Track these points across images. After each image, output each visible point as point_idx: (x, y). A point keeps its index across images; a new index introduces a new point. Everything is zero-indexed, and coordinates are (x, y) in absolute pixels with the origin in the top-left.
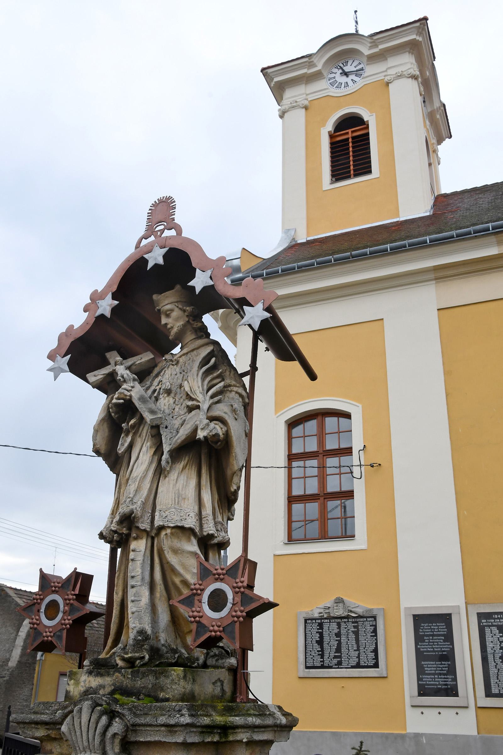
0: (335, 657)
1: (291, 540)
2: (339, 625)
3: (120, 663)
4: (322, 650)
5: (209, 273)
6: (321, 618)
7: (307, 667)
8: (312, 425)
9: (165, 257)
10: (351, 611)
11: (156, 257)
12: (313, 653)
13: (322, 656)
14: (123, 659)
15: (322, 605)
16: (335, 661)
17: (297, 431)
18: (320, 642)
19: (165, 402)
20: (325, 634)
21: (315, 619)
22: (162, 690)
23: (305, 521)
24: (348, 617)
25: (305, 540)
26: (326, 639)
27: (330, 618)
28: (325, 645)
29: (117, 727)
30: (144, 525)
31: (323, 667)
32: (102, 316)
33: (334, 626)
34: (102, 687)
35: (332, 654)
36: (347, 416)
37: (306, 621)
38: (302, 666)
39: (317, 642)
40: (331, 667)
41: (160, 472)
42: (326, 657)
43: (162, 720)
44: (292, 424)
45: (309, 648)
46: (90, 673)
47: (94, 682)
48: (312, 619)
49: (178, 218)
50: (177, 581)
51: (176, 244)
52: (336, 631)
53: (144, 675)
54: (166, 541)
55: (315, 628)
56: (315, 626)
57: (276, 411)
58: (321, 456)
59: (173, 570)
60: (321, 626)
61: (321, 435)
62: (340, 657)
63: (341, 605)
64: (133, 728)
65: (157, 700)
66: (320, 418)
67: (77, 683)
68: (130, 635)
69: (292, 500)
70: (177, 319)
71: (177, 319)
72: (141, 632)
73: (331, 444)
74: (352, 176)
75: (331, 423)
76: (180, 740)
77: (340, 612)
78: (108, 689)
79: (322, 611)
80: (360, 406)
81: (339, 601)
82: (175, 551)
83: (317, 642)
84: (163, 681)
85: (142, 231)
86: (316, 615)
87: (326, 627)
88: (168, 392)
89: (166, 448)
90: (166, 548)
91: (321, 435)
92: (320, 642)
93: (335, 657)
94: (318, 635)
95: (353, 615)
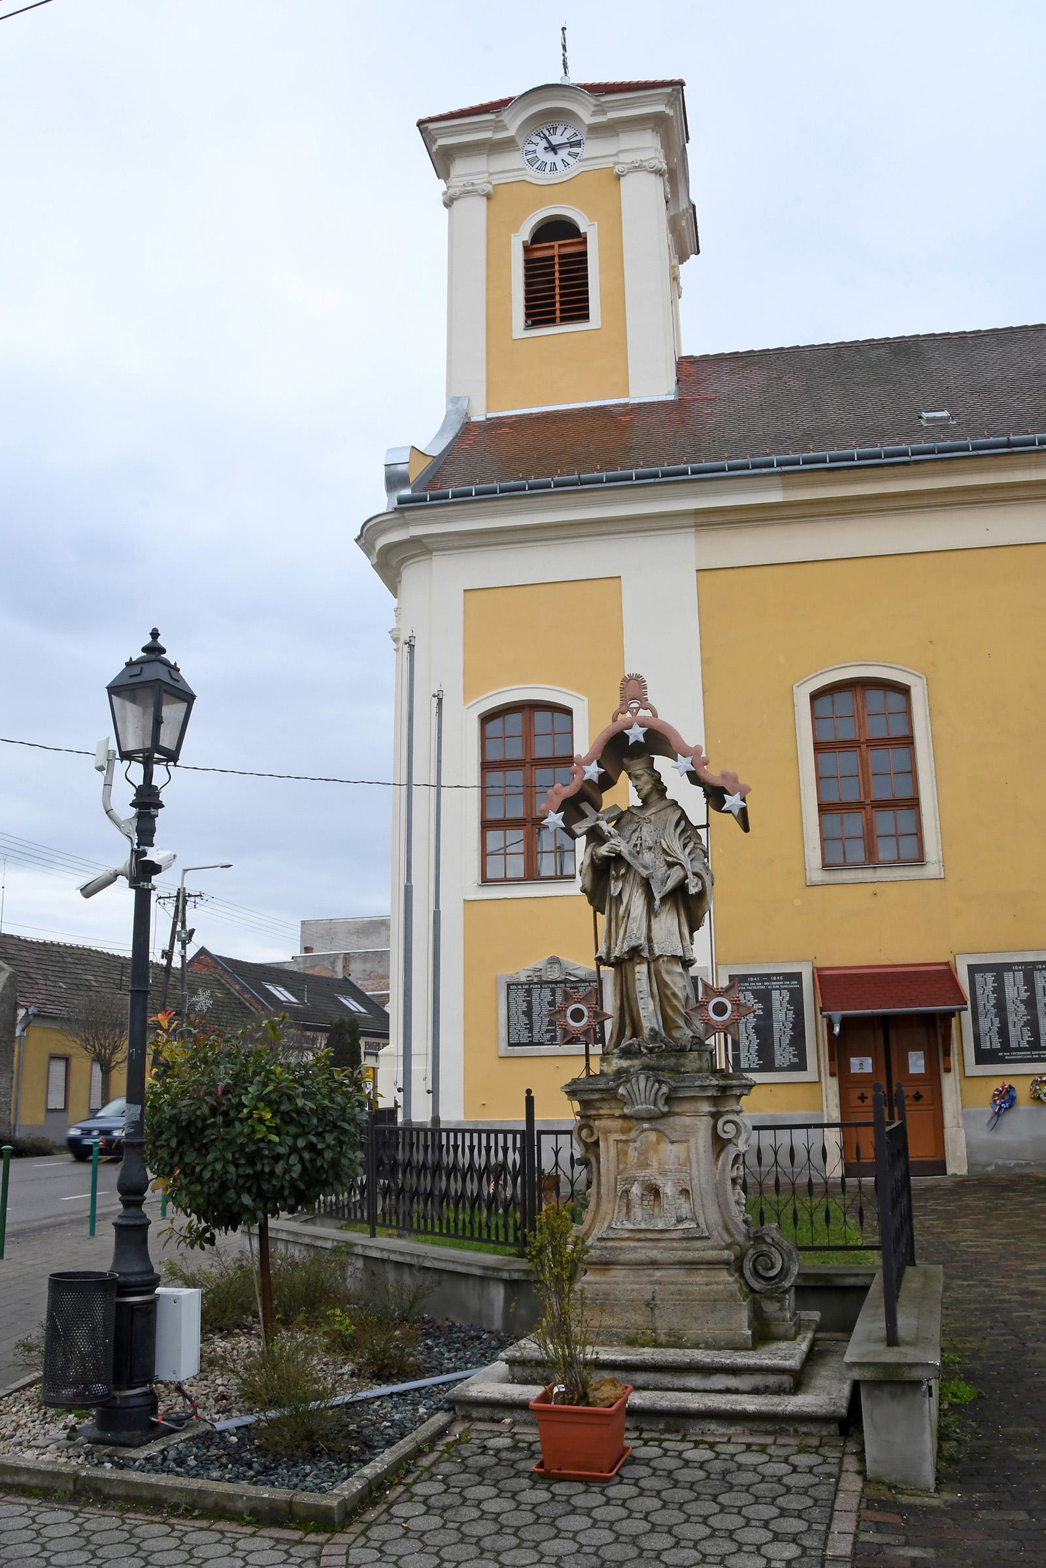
0: (548, 1031)
1: (485, 881)
2: (553, 992)
3: (645, 1051)
4: (531, 1023)
5: (690, 759)
6: (530, 983)
7: (510, 1045)
8: (515, 720)
9: (645, 735)
10: (570, 974)
11: (636, 734)
12: (518, 1027)
13: (531, 1030)
14: (646, 1048)
15: (531, 966)
16: (548, 1036)
17: (494, 726)
18: (528, 1013)
19: (648, 857)
20: (535, 1003)
21: (522, 984)
22: (683, 1066)
23: (505, 854)
24: (565, 981)
25: (506, 881)
26: (536, 1009)
27: (542, 983)
28: (535, 1017)
29: (665, 1089)
30: (645, 954)
31: (531, 1043)
32: (589, 781)
33: (547, 993)
34: (631, 1066)
35: (544, 1028)
36: (568, 712)
37: (509, 986)
38: (504, 1044)
39: (524, 1012)
40: (542, 1044)
41: (651, 912)
42: (535, 1032)
43: (698, 1083)
44: (487, 718)
45: (514, 1020)
46: (621, 1058)
47: (625, 1063)
48: (517, 985)
49: (652, 698)
50: (669, 993)
51: (653, 723)
52: (550, 998)
53: (666, 1058)
54: (663, 966)
55: (521, 994)
56: (522, 993)
57: (466, 699)
58: (528, 765)
59: (666, 985)
60: (529, 992)
61: (528, 736)
62: (554, 1031)
63: (556, 966)
64: (674, 1089)
65: (680, 1072)
66: (527, 711)
67: (610, 1064)
68: (646, 1032)
69: (487, 825)
70: (646, 783)
71: (646, 783)
72: (652, 1030)
73: (542, 749)
74: (558, 320)
75: (541, 719)
76: (710, 1094)
77: (555, 975)
78: (637, 1068)
79: (530, 973)
80: (586, 699)
81: (554, 961)
82: (669, 972)
83: (524, 1012)
84: (682, 1061)
85: (616, 704)
86: (523, 979)
87: (535, 994)
88: (650, 849)
89: (658, 896)
90: (662, 971)
91: (528, 736)
92: (528, 1013)
93: (548, 1031)
94: (525, 1004)
95: (573, 979)
